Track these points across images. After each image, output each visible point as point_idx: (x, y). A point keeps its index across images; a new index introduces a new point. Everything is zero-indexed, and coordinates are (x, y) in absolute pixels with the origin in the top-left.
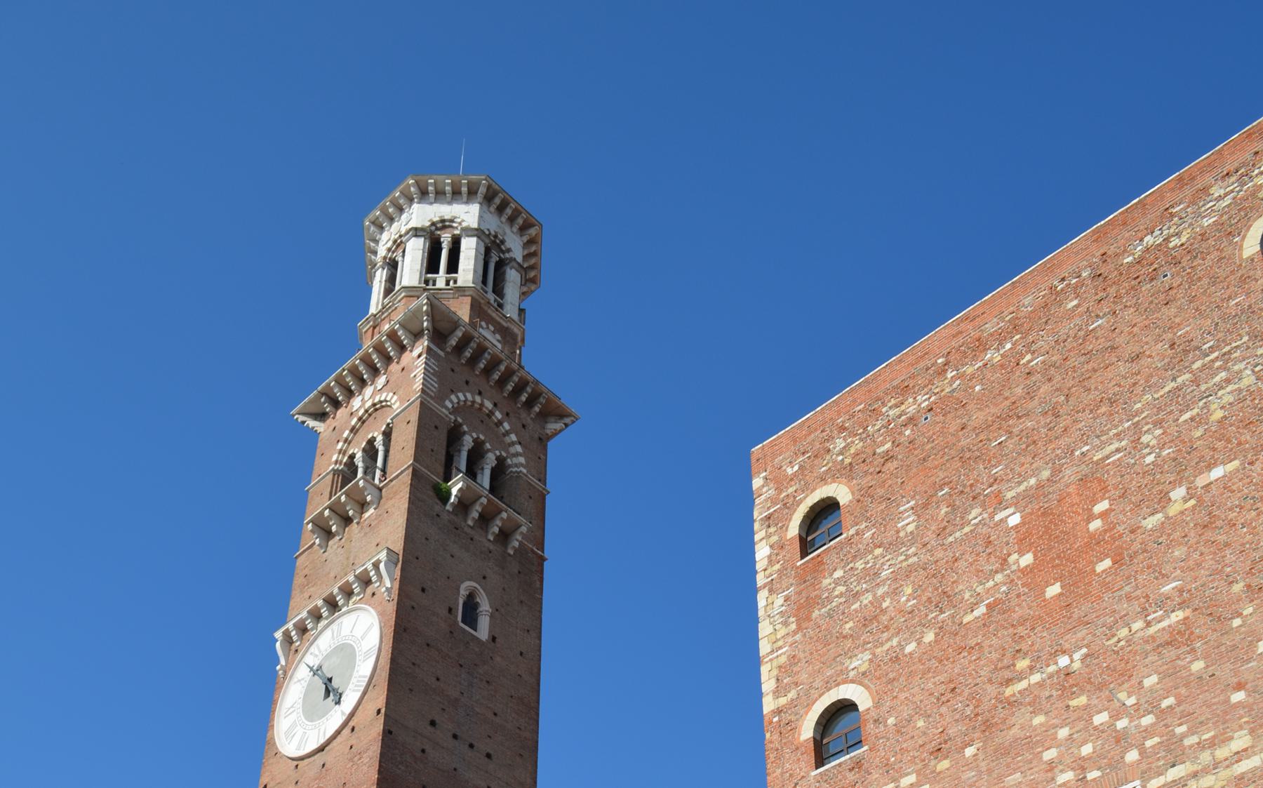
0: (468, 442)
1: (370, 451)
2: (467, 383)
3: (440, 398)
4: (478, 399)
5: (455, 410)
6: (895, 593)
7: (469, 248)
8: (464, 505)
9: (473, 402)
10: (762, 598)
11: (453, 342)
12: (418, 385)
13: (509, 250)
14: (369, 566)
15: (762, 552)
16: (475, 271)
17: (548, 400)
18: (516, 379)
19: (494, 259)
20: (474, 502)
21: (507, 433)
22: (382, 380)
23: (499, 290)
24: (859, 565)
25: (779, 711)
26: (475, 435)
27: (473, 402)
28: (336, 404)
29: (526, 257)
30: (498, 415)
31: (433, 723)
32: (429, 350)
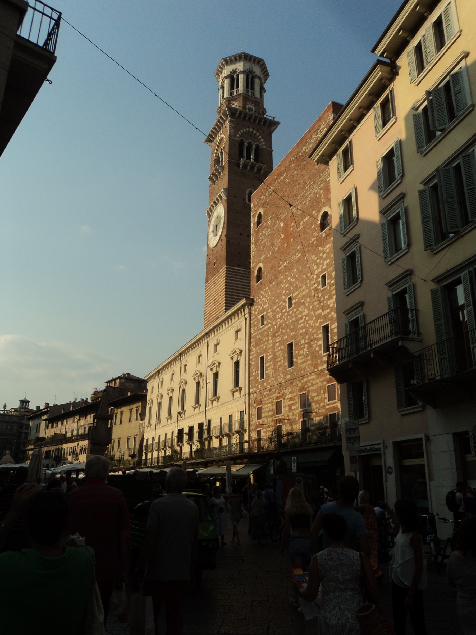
0: (246, 144)
1: (222, 153)
2: (244, 126)
3: (235, 135)
4: (247, 129)
5: (241, 136)
6: (267, 241)
7: (241, 77)
8: (245, 166)
9: (246, 131)
10: (252, 237)
11: (237, 115)
12: (228, 134)
13: (254, 72)
14: (220, 193)
15: (252, 225)
16: (243, 86)
17: (270, 121)
18: (258, 119)
19: (250, 76)
20: (248, 165)
21: (258, 136)
22: (222, 130)
23: (253, 88)
24: (263, 232)
25: (253, 268)
26: (248, 141)
27: (246, 131)
28: (214, 138)
29: (262, 70)
30: (255, 132)
31: (241, 234)
32: (230, 121)
